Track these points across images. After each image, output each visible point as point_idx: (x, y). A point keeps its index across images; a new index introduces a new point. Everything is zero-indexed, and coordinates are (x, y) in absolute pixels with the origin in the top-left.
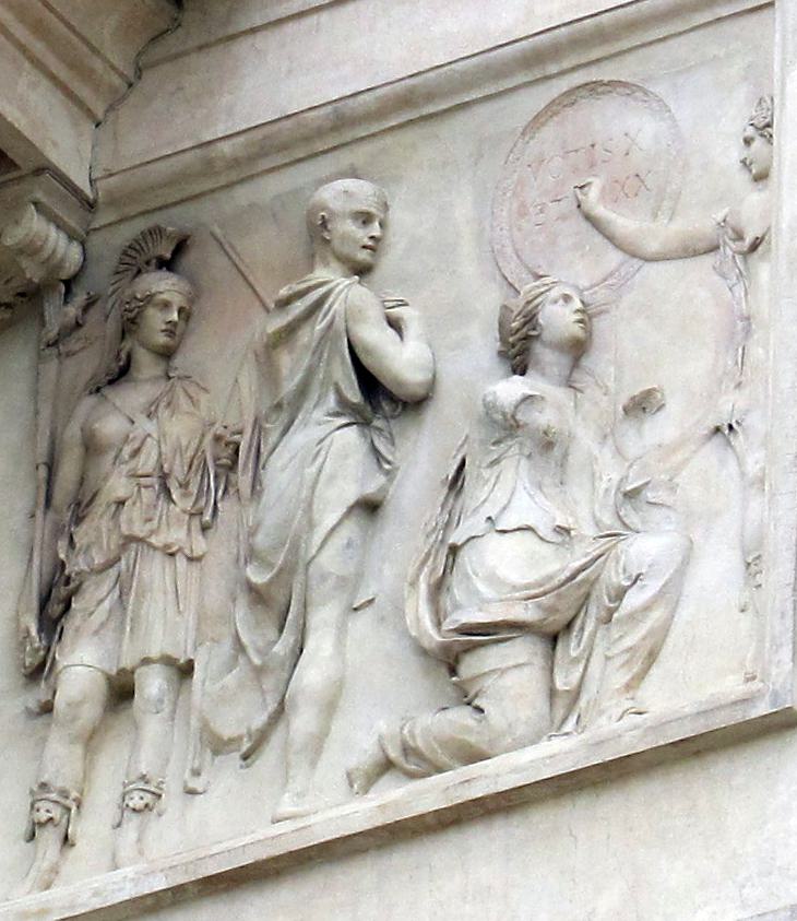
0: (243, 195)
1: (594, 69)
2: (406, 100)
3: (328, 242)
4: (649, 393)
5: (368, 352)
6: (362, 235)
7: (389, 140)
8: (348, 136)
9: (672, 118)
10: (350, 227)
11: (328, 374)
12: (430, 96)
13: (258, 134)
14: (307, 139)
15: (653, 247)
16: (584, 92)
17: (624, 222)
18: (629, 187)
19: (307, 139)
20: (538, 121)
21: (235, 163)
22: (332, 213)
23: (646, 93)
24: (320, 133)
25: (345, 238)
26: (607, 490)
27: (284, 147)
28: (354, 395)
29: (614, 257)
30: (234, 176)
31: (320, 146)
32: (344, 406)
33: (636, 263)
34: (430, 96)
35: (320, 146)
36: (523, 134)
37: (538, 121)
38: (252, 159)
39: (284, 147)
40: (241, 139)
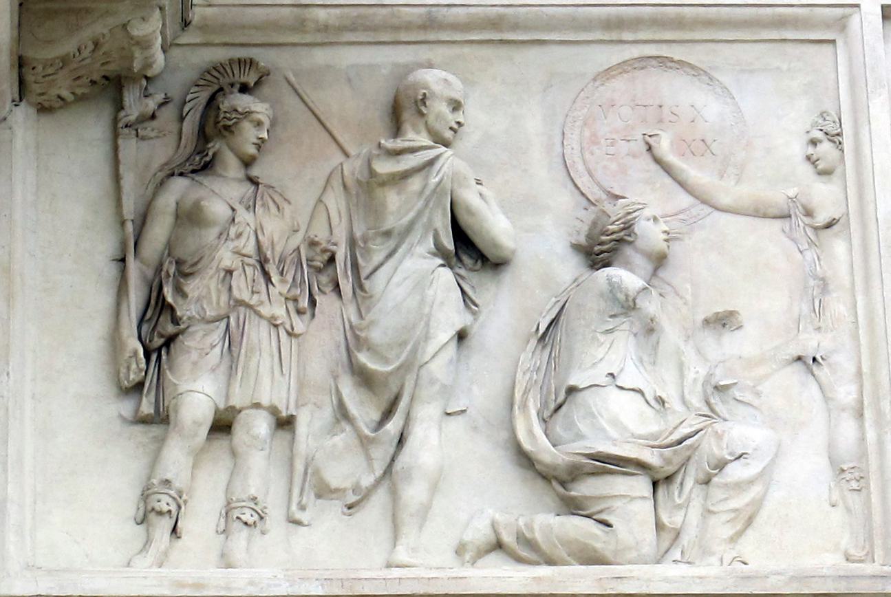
0: (320, 56)
1: (664, 46)
2: (495, 23)
3: (422, 114)
4: (732, 314)
5: (470, 212)
6: (452, 118)
7: (466, 50)
8: (432, 36)
9: (736, 104)
10: (444, 109)
11: (430, 220)
12: (515, 27)
13: (354, 12)
14: (396, 28)
15: (725, 200)
16: (654, 62)
17: (694, 173)
18: (699, 147)
19: (396, 28)
20: (607, 74)
21: (325, 28)
22: (433, 94)
23: (711, 79)
24: (408, 26)
25: (439, 116)
26: (695, 380)
27: (375, 29)
28: (449, 244)
29: (685, 200)
30: (319, 38)
31: (404, 37)
32: (440, 251)
33: (707, 209)
34: (515, 27)
35: (404, 37)
36: (595, 80)
37: (607, 74)
38: (342, 29)
39: (375, 29)
40: (338, 11)
